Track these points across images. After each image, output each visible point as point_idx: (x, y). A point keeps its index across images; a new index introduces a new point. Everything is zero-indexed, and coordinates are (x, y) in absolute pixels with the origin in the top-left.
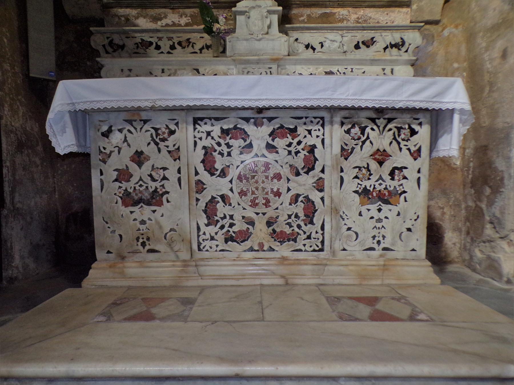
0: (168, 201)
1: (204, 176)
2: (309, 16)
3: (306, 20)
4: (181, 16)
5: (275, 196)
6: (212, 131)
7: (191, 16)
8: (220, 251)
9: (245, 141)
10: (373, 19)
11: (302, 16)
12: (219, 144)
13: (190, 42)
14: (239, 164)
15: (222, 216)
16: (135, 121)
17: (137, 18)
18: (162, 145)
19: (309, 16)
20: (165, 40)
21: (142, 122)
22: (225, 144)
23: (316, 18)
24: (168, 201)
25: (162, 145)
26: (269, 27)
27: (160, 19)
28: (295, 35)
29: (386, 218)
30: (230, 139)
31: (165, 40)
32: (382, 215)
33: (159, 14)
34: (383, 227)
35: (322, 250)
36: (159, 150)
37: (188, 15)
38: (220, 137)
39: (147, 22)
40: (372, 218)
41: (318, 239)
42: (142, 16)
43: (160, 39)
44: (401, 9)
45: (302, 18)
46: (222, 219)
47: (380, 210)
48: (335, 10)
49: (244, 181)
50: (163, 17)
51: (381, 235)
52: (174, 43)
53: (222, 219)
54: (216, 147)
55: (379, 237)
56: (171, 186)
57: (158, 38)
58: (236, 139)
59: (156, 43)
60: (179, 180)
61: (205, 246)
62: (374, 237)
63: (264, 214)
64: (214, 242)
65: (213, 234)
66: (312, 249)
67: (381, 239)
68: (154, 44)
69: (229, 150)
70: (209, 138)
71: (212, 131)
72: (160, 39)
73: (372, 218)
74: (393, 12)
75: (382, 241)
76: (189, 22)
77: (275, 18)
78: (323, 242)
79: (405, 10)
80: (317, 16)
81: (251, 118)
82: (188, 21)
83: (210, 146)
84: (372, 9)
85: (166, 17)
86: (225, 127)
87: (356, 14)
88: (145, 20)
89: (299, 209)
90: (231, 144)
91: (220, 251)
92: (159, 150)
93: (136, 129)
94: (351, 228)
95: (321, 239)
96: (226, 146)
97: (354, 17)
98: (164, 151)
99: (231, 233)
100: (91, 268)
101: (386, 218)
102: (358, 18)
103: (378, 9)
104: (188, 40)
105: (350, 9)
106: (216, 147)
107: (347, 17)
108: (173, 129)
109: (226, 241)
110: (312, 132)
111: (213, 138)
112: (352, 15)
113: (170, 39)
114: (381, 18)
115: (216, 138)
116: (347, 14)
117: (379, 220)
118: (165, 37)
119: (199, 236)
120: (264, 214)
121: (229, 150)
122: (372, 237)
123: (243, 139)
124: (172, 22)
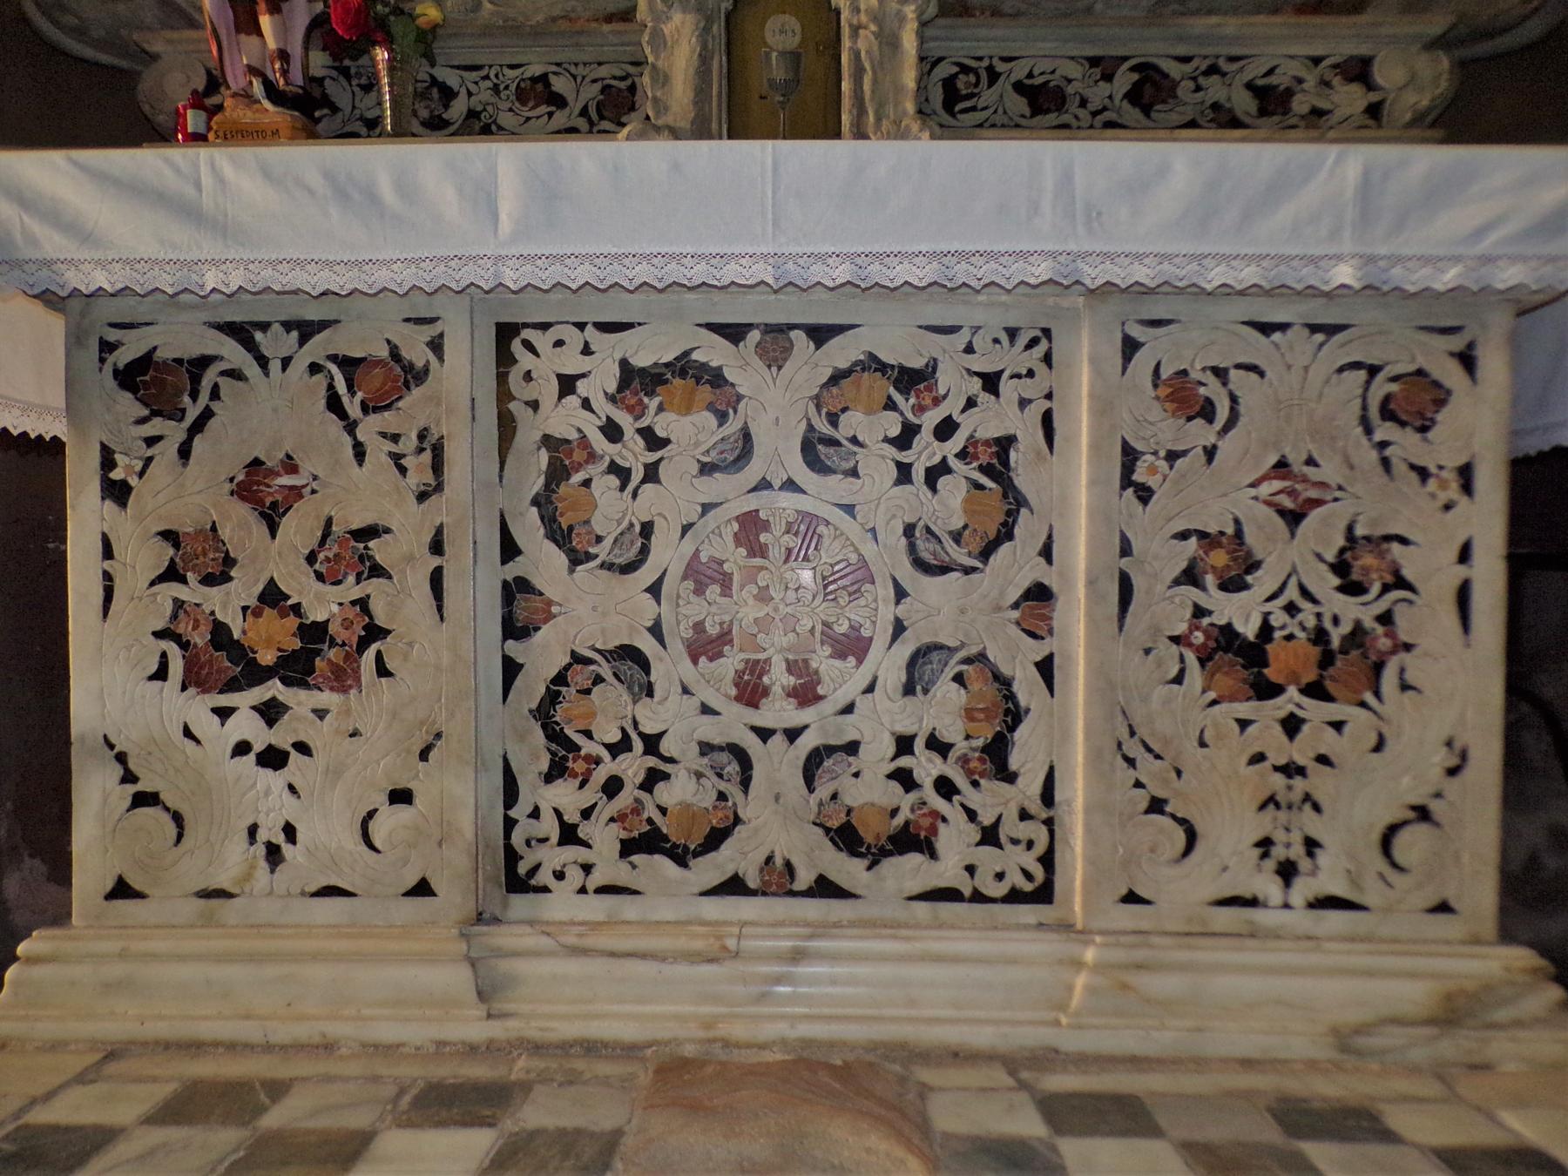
0: (383, 671)
1: (543, 562)
5: (841, 655)
6: (583, 376)
8: (601, 890)
9: (722, 417)
12: (612, 432)
14: (694, 518)
15: (614, 736)
16: (264, 327)
18: (368, 429)
21: (295, 334)
22: (639, 431)
24: (383, 671)
25: (368, 429)
29: (1323, 760)
30: (660, 409)
32: (1300, 751)
34: (1307, 797)
35: (1044, 894)
36: (360, 453)
38: (612, 399)
40: (1259, 758)
41: (1030, 845)
46: (616, 749)
47: (1292, 725)
49: (713, 591)
51: (1297, 838)
53: (616, 749)
54: (599, 442)
55: (1288, 845)
56: (400, 602)
58: (687, 409)
60: (436, 579)
61: (537, 867)
62: (1265, 844)
63: (792, 735)
64: (572, 853)
65: (572, 817)
66: (1001, 890)
67: (1297, 852)
69: (652, 457)
70: (572, 401)
71: (583, 376)
73: (1259, 758)
75: (1304, 864)
78: (1047, 860)
81: (750, 326)
83: (574, 436)
86: (642, 361)
89: (944, 708)
90: (660, 433)
91: (601, 890)
92: (360, 453)
93: (263, 362)
94: (1165, 801)
95: (1040, 848)
96: (641, 442)
98: (379, 451)
99: (651, 811)
100: (15, 958)
101: (1323, 760)
106: (599, 442)
108: (420, 365)
109: (628, 848)
110: (1006, 386)
111: (586, 404)
115: (599, 403)
117: (1291, 770)
119: (510, 824)
120: (792, 735)
121: (652, 457)
122: (1258, 844)
123: (710, 407)
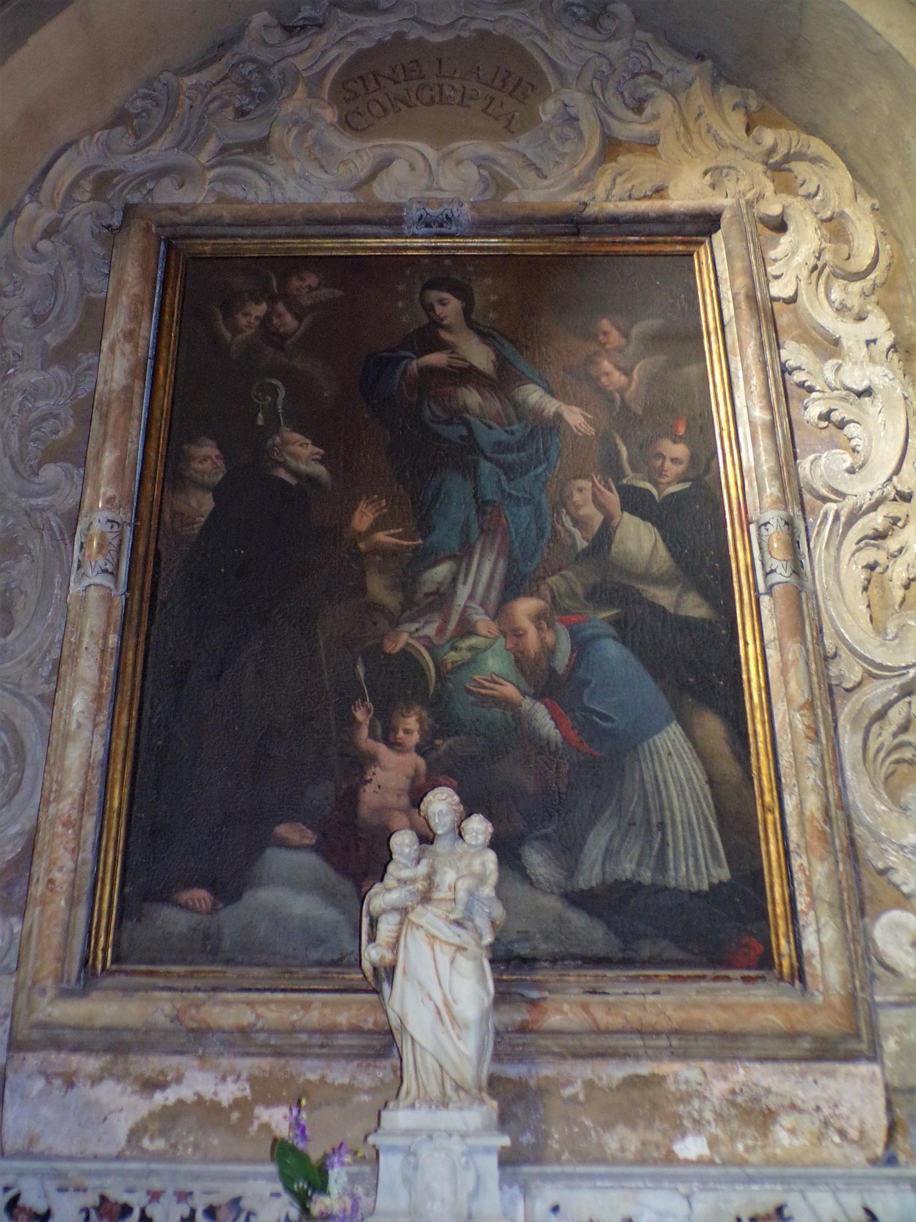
2: (589, 1085)
3: (581, 1097)
4: (224, 1079)
7: (253, 1080)
10: (777, 1095)
11: (570, 1083)
13: (239, 1211)
17: (96, 1080)
19: (589, 1085)
20: (169, 1199)
23: (610, 1089)
26: (474, 1195)
27: (162, 1086)
28: (549, 1194)
31: (169, 1199)
33: (162, 1072)
37: (244, 1075)
39: (123, 1092)
42: (111, 1075)
43: (155, 1196)
44: (851, 1067)
45: (568, 1092)
48: (667, 1068)
50: (172, 1080)
52: (193, 1212)
57: (148, 1192)
59: (143, 1211)
68: (136, 1213)
72: (155, 1196)
74: (831, 1075)
76: (245, 1098)
77: (490, 1164)
79: (864, 1068)
80: (615, 1083)
82: (239, 1094)
84: (769, 1066)
85: (179, 1080)
87: (725, 1078)
88: (119, 1088)
97: (719, 1088)
102: (733, 1092)
103: (786, 1067)
104: (236, 1202)
105: (708, 1065)
107: (701, 1089)
112: (715, 1082)
113: (183, 1196)
114: (800, 1093)
116: (701, 1078)
118: (170, 1191)
124: (197, 1094)
